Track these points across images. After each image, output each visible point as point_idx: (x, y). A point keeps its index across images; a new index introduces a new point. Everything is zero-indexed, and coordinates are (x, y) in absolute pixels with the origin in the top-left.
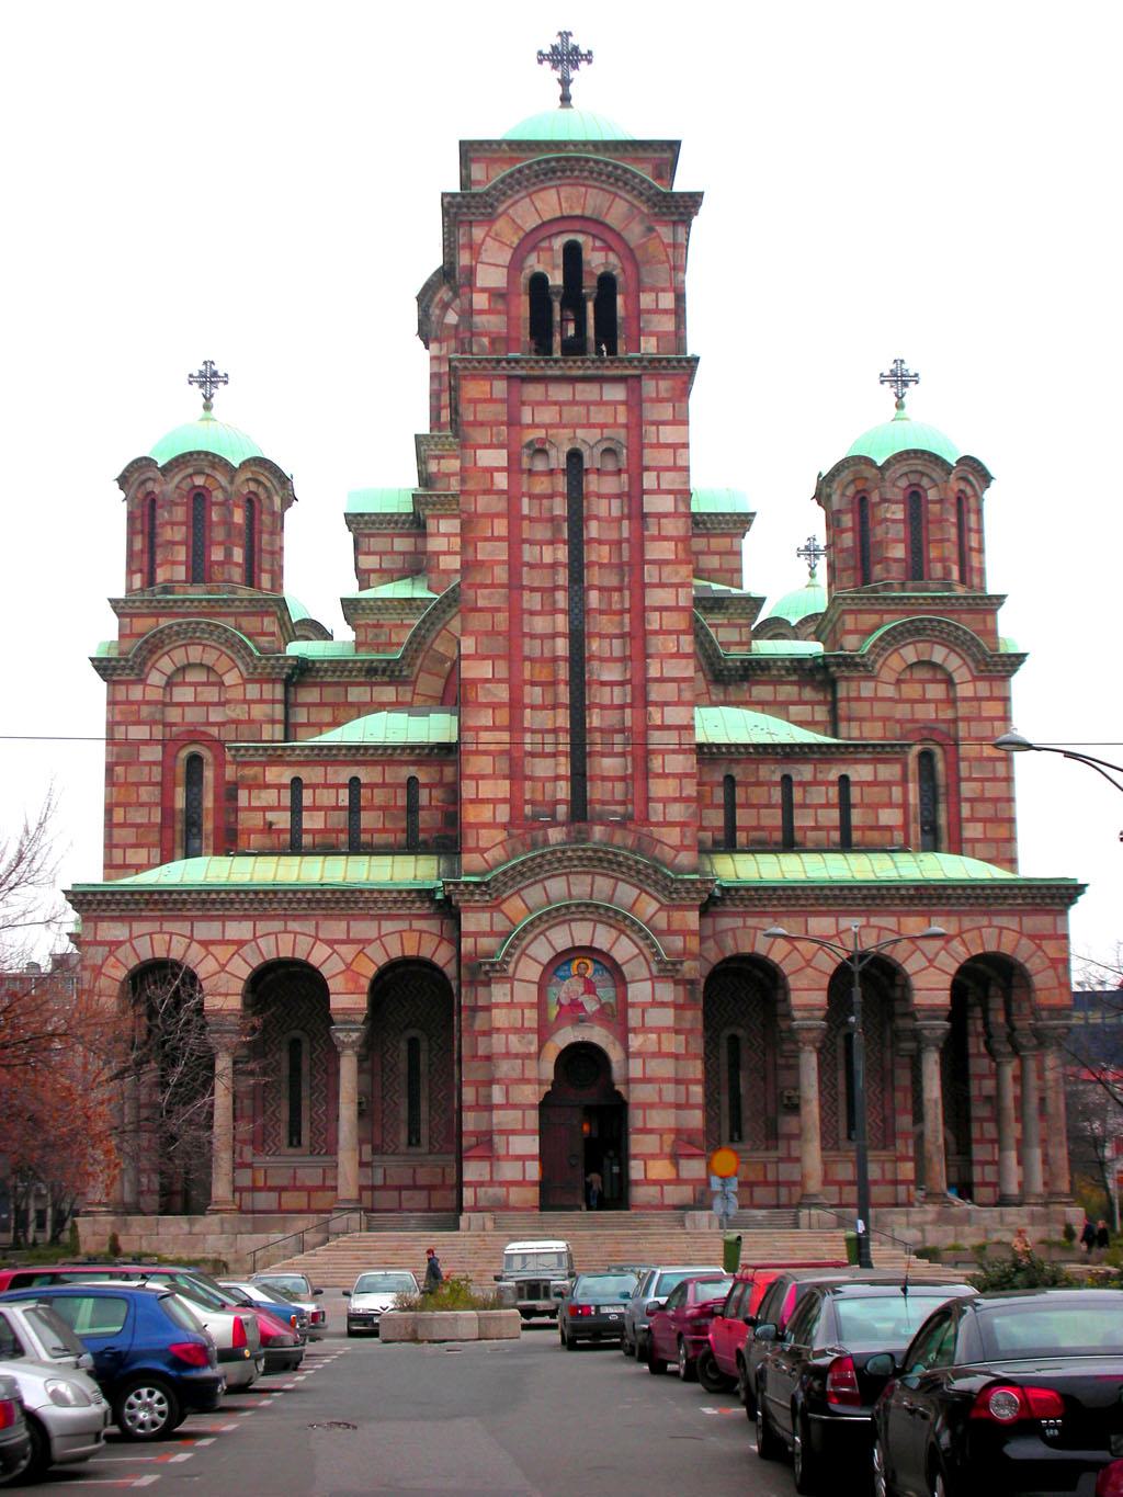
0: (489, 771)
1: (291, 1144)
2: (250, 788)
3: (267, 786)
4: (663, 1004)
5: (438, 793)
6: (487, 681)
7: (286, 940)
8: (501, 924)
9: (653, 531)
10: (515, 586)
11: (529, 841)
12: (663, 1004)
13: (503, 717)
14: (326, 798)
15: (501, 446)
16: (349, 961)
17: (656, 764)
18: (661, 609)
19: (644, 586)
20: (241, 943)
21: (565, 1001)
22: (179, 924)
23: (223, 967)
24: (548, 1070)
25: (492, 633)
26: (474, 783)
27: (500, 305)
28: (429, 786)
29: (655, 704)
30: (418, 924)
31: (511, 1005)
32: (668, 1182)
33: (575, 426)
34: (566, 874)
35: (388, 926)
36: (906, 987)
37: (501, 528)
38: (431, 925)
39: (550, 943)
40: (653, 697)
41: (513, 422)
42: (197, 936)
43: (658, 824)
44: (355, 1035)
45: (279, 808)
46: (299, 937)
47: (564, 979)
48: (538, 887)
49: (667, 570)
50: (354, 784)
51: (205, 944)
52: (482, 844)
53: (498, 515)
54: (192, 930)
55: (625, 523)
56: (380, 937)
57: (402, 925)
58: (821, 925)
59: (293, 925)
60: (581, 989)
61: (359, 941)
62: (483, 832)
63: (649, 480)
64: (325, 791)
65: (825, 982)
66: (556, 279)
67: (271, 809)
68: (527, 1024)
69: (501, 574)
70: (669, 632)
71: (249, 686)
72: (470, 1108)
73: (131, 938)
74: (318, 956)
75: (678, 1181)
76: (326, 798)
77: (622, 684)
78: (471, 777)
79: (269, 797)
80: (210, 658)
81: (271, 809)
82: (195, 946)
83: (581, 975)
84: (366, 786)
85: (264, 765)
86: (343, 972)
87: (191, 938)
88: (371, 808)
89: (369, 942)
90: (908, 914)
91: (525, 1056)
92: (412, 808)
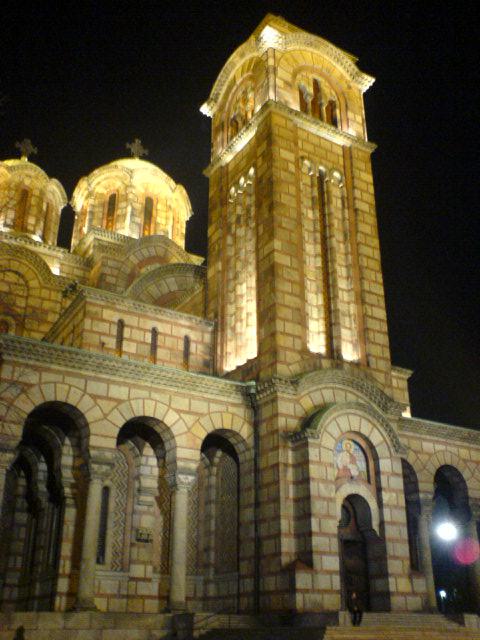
0: (290, 317)
1: (98, 562)
2: (92, 319)
3: (104, 320)
4: (397, 475)
5: (200, 347)
6: (287, 267)
7: (150, 404)
8: (300, 413)
9: (360, 218)
10: (299, 224)
11: (312, 364)
12: (397, 475)
13: (297, 289)
14: (138, 335)
15: (291, 151)
16: (190, 424)
17: (371, 335)
18: (368, 257)
19: (358, 244)
20: (119, 401)
21: (341, 467)
22: (77, 380)
23: (105, 416)
24: (337, 511)
25: (290, 242)
26: (282, 323)
27: (288, 88)
28: (196, 342)
29: (369, 304)
30: (231, 409)
31: (320, 463)
32: (408, 594)
33: (322, 158)
34: (333, 388)
35: (214, 407)
36: (465, 488)
37: (292, 190)
38: (241, 412)
39: (338, 425)
40: (367, 300)
41: (296, 144)
42: (89, 390)
43: (375, 370)
44: (191, 478)
45: (109, 335)
46: (159, 405)
47: (340, 451)
48: (319, 393)
49: (369, 238)
50: (155, 332)
51: (95, 397)
52: (288, 360)
53: (292, 183)
54: (86, 386)
55: (346, 211)
56: (209, 413)
57: (224, 408)
58: (428, 446)
59: (155, 396)
60: (348, 460)
61: (196, 414)
62: (288, 353)
63: (357, 193)
64: (138, 332)
65: (432, 479)
66: (310, 90)
67: (104, 334)
68: (329, 477)
69: (294, 214)
70: (372, 270)
71: (44, 290)
72: (286, 535)
73: (40, 384)
74: (170, 419)
75: (414, 593)
76: (138, 335)
77: (349, 291)
78: (281, 319)
79: (104, 327)
80: (23, 270)
81: (104, 334)
82: (87, 396)
83: (348, 451)
84: (161, 334)
85: (103, 307)
86: (186, 433)
87: (85, 391)
88: (164, 347)
89: (202, 415)
90: (462, 447)
91: (331, 500)
92: (187, 353)
